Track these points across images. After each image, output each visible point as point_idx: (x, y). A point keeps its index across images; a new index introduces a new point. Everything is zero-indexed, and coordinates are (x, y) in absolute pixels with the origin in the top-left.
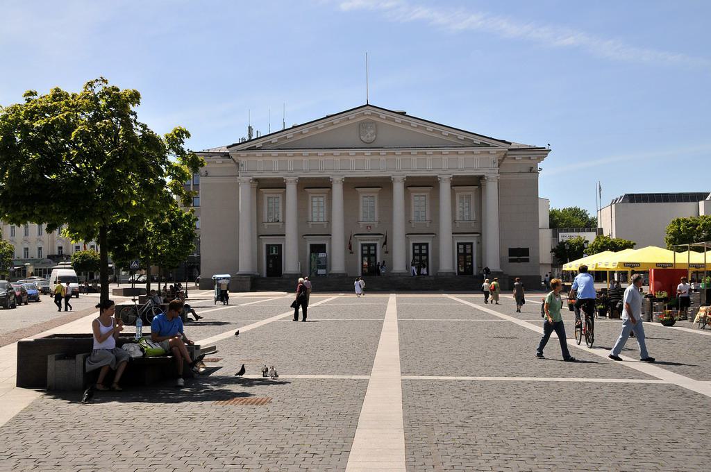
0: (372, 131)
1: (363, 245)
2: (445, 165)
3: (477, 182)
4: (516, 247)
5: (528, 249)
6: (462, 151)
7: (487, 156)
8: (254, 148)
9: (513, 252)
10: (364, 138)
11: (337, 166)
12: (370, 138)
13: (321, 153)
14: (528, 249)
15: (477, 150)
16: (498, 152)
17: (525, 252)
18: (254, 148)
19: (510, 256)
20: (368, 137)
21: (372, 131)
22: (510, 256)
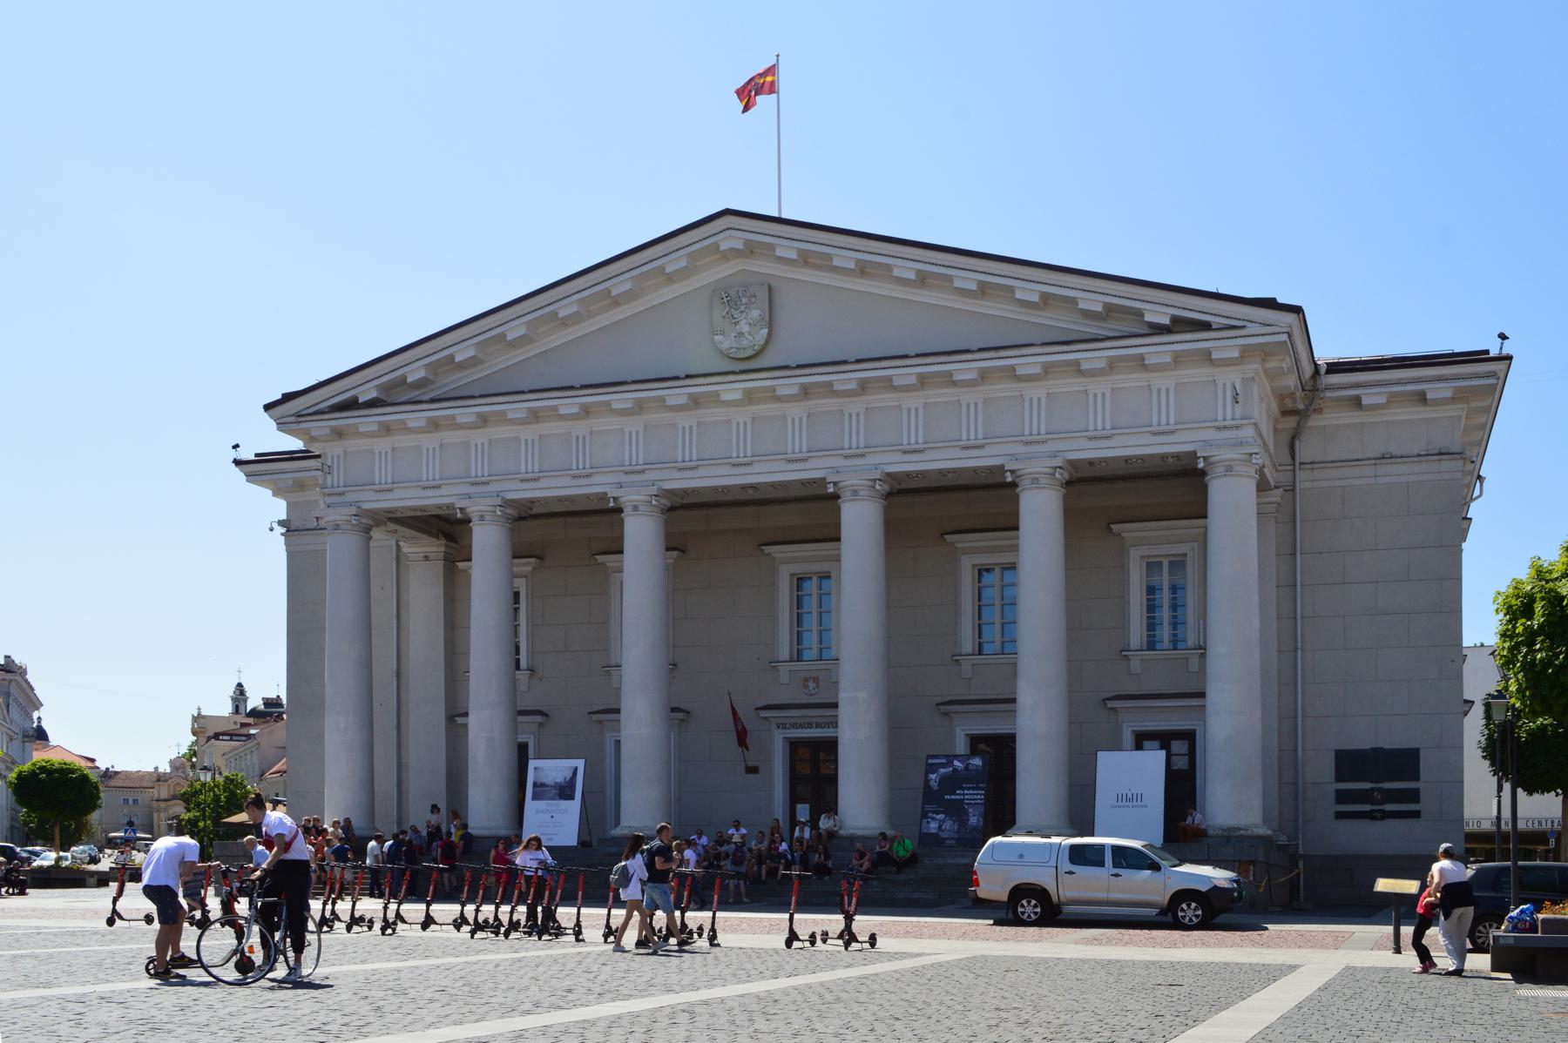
0: (755, 313)
1: (794, 746)
2: (1038, 426)
3: (1178, 486)
4: (1362, 739)
5: (1418, 750)
6: (1093, 357)
7: (1200, 373)
8: (351, 405)
9: (1350, 763)
10: (726, 342)
11: (627, 456)
12: (745, 343)
13: (569, 405)
14: (1418, 750)
15: (1158, 351)
16: (1246, 352)
17: (1404, 762)
18: (351, 405)
19: (1339, 778)
20: (741, 334)
21: (755, 313)
22: (1339, 778)
